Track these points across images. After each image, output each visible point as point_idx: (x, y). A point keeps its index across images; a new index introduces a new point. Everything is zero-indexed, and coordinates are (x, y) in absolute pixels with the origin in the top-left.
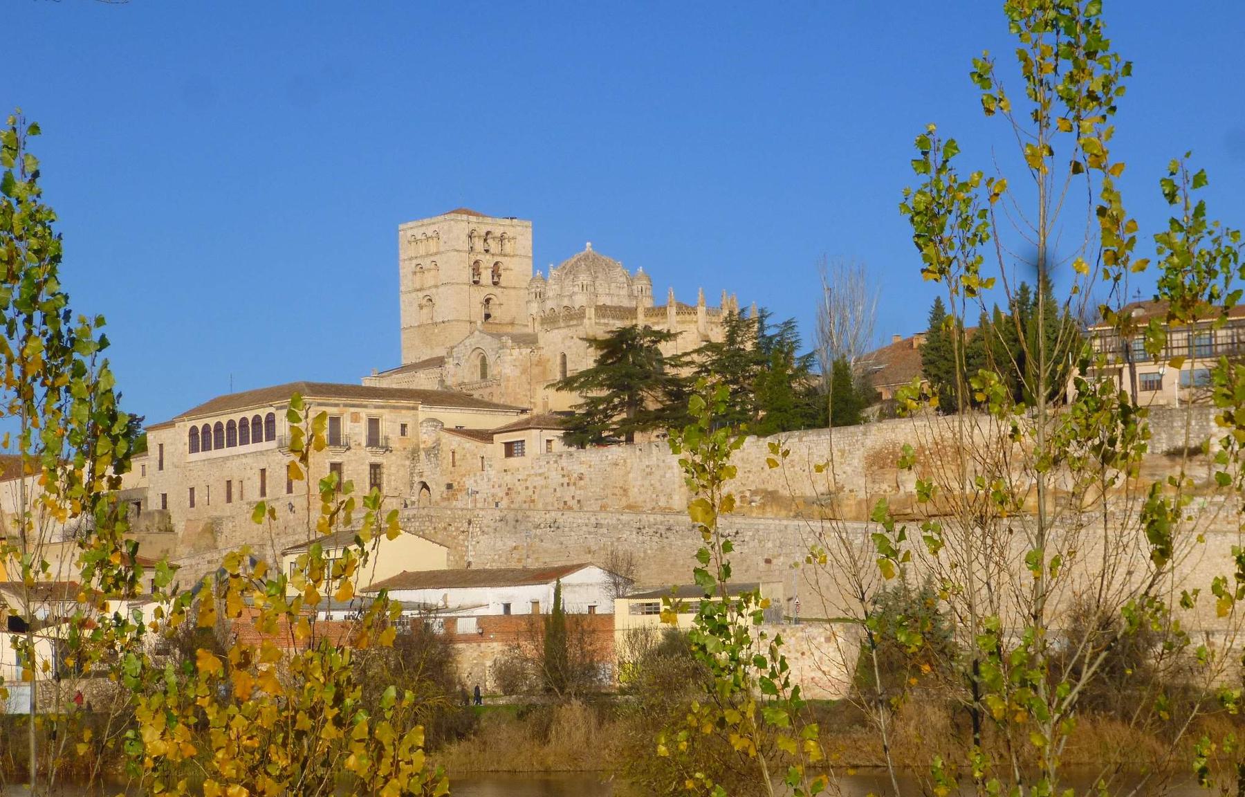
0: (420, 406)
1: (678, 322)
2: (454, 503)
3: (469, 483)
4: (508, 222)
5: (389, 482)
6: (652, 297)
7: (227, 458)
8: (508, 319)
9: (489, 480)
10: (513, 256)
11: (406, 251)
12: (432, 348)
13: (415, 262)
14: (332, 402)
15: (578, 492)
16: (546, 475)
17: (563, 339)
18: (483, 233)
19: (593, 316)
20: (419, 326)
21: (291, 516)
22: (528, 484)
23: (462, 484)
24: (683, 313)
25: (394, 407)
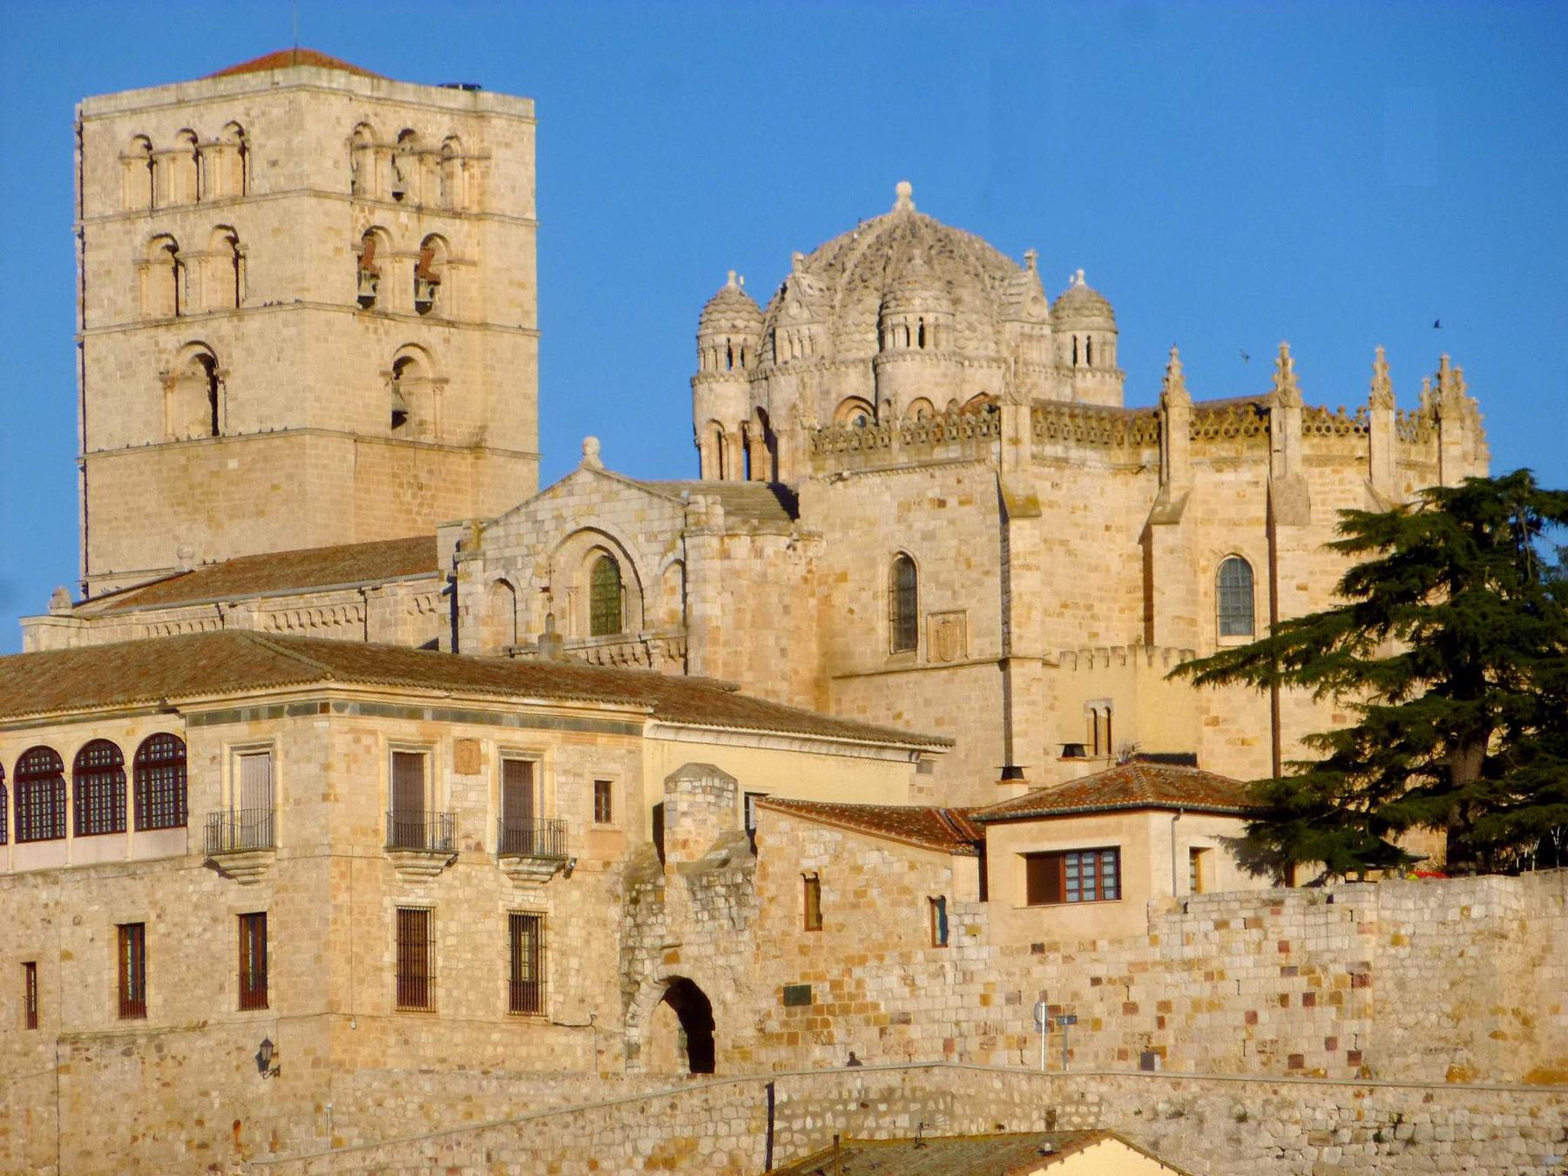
0: (650, 722)
1: (1307, 460)
2: (817, 1052)
4: (461, 98)
5: (563, 975)
6: (1121, 371)
8: (460, 433)
9: (968, 977)
10: (481, 216)
12: (211, 521)
13: (145, 227)
14: (401, 701)
15: (1351, 1026)
16: (1214, 965)
17: (905, 507)
18: (390, 136)
19: (1026, 433)
20: (161, 447)
21: (263, 1085)
22: (1137, 994)
23: (849, 986)
24: (1326, 431)
25: (577, 725)
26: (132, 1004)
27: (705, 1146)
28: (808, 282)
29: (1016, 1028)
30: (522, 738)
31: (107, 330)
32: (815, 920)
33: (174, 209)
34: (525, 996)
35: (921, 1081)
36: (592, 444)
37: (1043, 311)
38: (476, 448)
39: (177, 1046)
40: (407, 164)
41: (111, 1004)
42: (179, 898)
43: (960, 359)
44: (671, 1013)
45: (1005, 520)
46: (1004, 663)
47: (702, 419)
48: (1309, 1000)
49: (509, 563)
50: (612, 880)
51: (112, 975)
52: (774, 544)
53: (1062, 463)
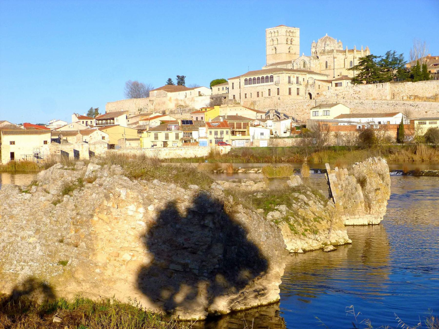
3: (324, 93)
7: (258, 86)
8: (294, 53)
11: (268, 35)
13: (271, 38)
15: (359, 95)
17: (327, 58)
21: (279, 101)
22: (343, 93)
25: (302, 74)
26: (269, 95)
30: (298, 75)
32: (319, 88)
34: (298, 94)
35: (327, 100)
36: (303, 53)
37: (337, 43)
38: (295, 54)
40: (290, 33)
41: (268, 95)
50: (305, 85)
52: (317, 61)
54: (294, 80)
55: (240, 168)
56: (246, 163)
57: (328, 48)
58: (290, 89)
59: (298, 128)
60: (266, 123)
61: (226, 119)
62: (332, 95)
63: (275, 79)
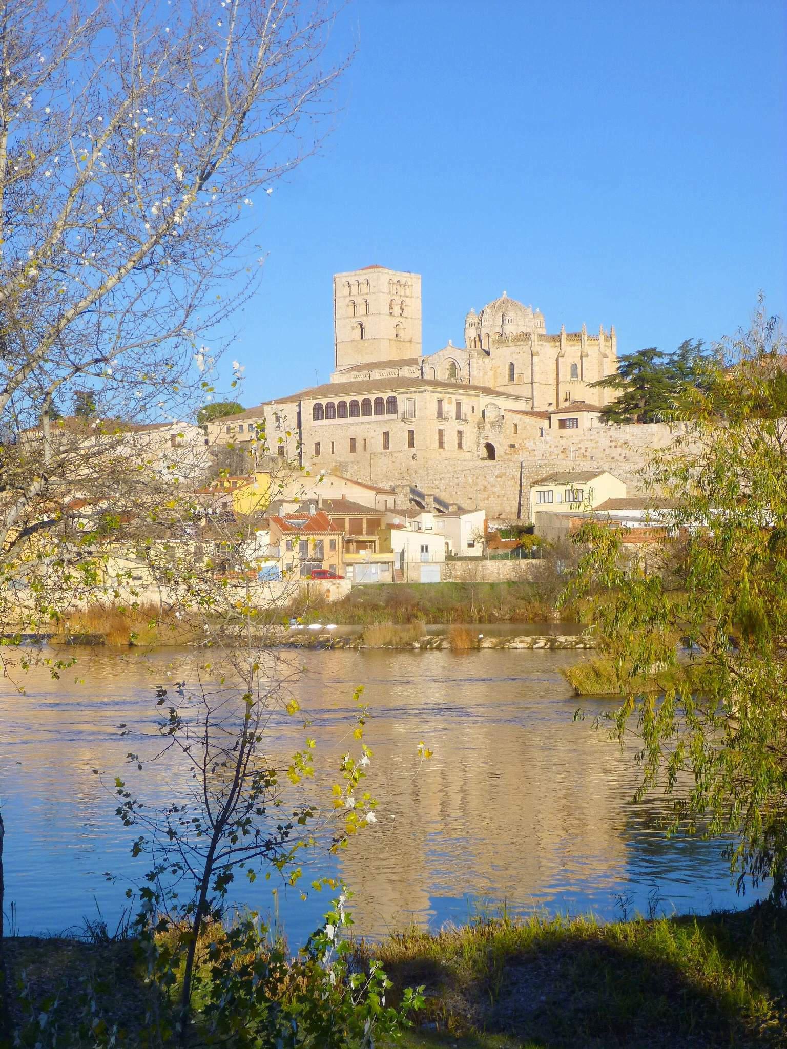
1: (588, 345)
2: (516, 456)
3: (530, 444)
4: (408, 274)
7: (352, 424)
8: (407, 339)
11: (342, 291)
13: (348, 299)
17: (512, 354)
18: (395, 281)
19: (536, 340)
21: (413, 462)
23: (523, 444)
25: (468, 395)
26: (386, 447)
27: (508, 474)
28: (488, 311)
29: (557, 452)
30: (459, 398)
31: (341, 318)
32: (516, 432)
33: (354, 295)
34: (460, 446)
36: (450, 341)
38: (411, 341)
39: (395, 455)
40: (398, 287)
42: (396, 427)
43: (518, 325)
44: (485, 449)
45: (532, 356)
46: (532, 384)
47: (466, 337)
48: (616, 447)
49: (433, 364)
51: (382, 442)
52: (487, 360)
53: (542, 345)
54: (449, 409)
55: (482, 636)
56: (404, 623)
57: (511, 329)
58: (441, 432)
59: (507, 533)
60: (416, 519)
61: (321, 509)
62: (552, 450)
63: (403, 404)
